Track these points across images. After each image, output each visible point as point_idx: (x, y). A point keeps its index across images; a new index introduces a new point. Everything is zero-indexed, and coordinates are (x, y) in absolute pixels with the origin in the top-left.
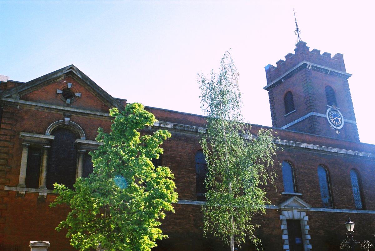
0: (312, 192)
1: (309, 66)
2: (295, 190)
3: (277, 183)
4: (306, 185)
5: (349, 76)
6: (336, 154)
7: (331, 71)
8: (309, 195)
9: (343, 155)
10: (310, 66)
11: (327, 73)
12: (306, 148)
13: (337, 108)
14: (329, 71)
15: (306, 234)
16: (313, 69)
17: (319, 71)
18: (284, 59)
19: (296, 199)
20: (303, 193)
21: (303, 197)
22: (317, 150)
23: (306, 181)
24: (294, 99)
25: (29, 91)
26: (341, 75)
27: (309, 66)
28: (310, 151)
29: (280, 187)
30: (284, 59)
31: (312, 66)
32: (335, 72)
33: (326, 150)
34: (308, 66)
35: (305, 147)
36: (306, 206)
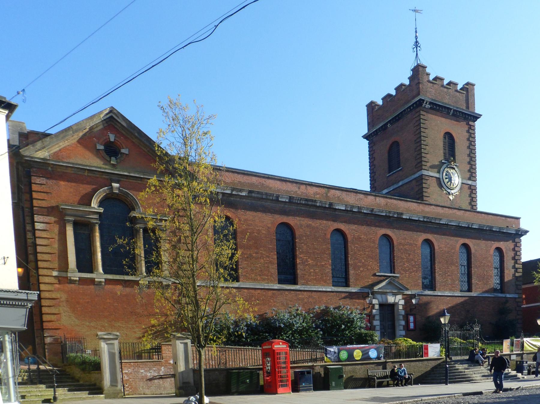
2: (391, 271)
3: (371, 263)
4: (405, 265)
5: (476, 117)
6: (446, 225)
8: (407, 276)
9: (454, 227)
12: (409, 219)
13: (455, 164)
15: (400, 319)
18: (394, 93)
19: (392, 281)
20: (401, 274)
21: (400, 278)
22: (423, 221)
23: (405, 260)
24: (401, 152)
25: (60, 146)
26: (467, 117)
28: (414, 223)
29: (374, 267)
30: (394, 93)
33: (434, 221)
35: (408, 218)
36: (403, 289)
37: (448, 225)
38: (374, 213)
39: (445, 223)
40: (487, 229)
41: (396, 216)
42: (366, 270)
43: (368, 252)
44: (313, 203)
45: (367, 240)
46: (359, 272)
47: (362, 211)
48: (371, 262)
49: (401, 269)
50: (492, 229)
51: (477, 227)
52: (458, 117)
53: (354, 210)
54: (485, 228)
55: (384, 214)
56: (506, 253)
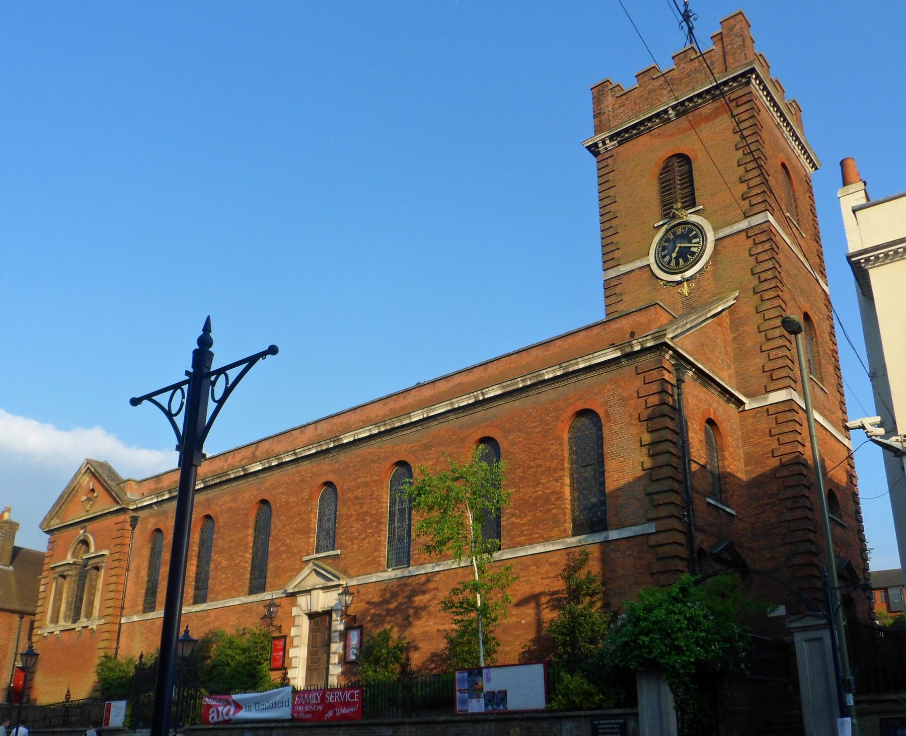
0: (364, 539)
1: (604, 143)
3: (299, 541)
7: (674, 107)
10: (608, 141)
11: (669, 120)
14: (671, 112)
16: (619, 142)
17: (639, 134)
21: (343, 556)
22: (380, 434)
23: (354, 518)
27: (604, 143)
31: (611, 138)
32: (690, 100)
33: (399, 424)
34: (600, 145)
35: (351, 439)
37: (429, 418)
38: (299, 456)
39: (421, 417)
40: (529, 383)
41: (331, 445)
42: (291, 555)
43: (297, 523)
44: (224, 479)
45: (298, 504)
46: (280, 563)
47: (284, 461)
48: (299, 539)
49: (346, 538)
50: (540, 379)
51: (499, 392)
52: (696, 107)
53: (273, 464)
54: (521, 385)
55: (314, 451)
56: (608, 415)
